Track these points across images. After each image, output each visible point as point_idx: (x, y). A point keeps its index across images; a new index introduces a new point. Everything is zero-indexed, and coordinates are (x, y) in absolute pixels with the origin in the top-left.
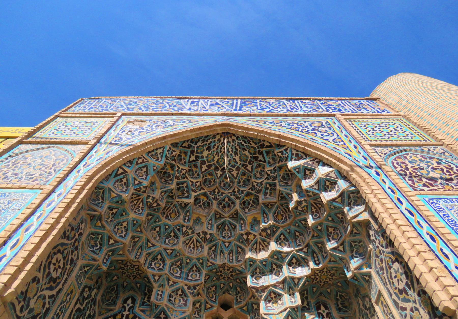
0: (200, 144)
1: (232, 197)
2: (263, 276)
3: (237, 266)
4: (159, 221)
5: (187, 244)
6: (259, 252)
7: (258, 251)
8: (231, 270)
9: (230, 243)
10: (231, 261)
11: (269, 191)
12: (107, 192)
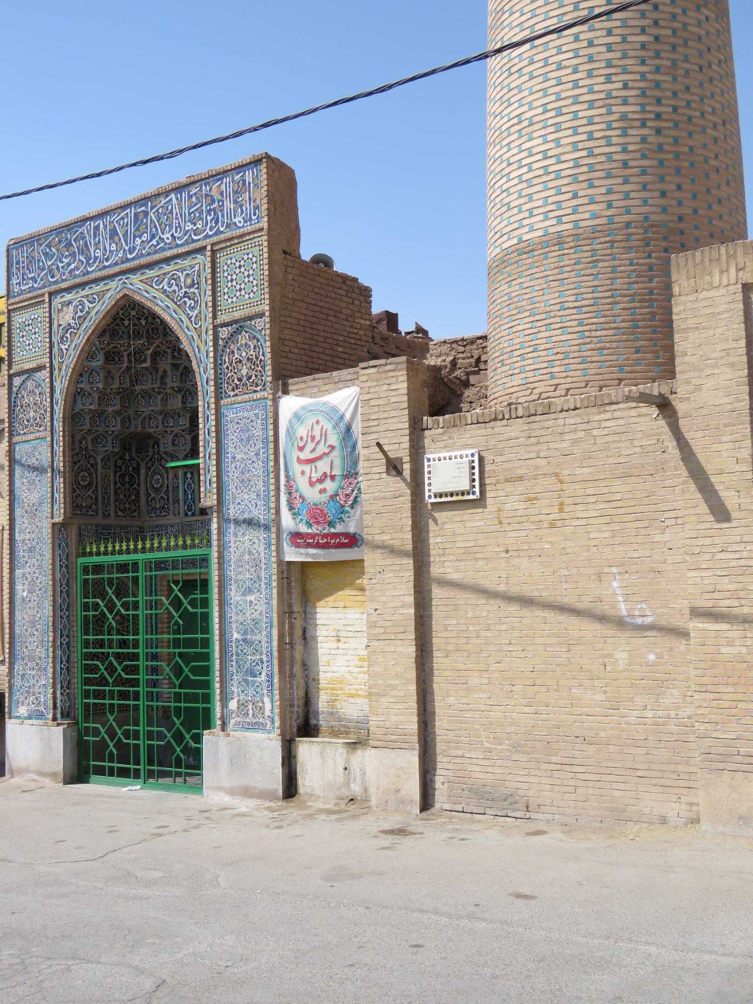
12: (81, 412)
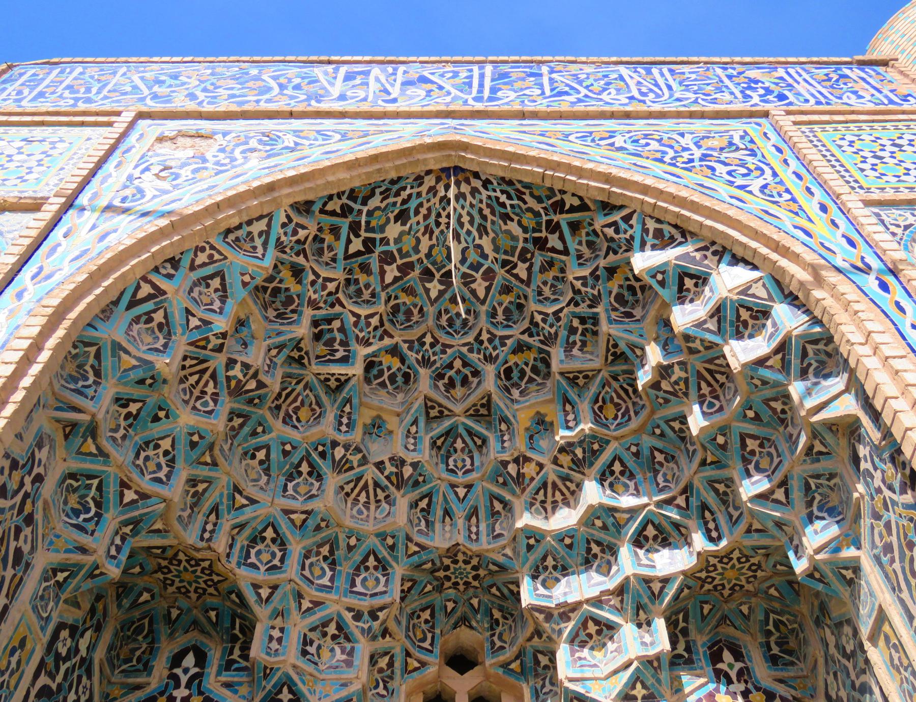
0: (375, 202)
1: (474, 357)
2: (564, 576)
3: (493, 550)
4: (264, 432)
5: (348, 494)
6: (554, 509)
7: (549, 508)
8: (475, 562)
9: (469, 487)
10: (474, 537)
11: (577, 337)
12: (107, 354)
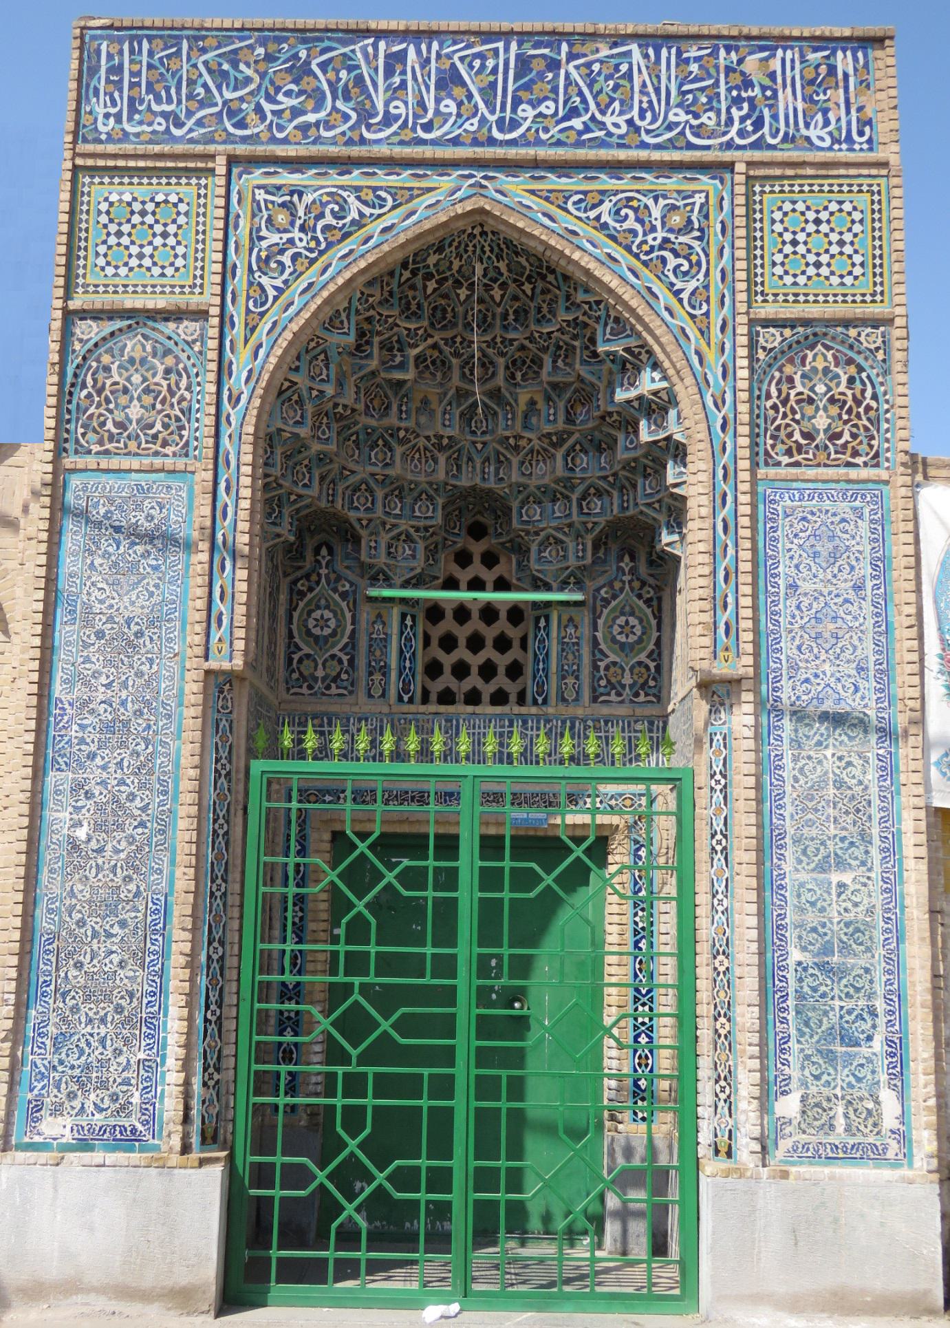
1: (490, 351)
9: (484, 444)
11: (562, 352)
